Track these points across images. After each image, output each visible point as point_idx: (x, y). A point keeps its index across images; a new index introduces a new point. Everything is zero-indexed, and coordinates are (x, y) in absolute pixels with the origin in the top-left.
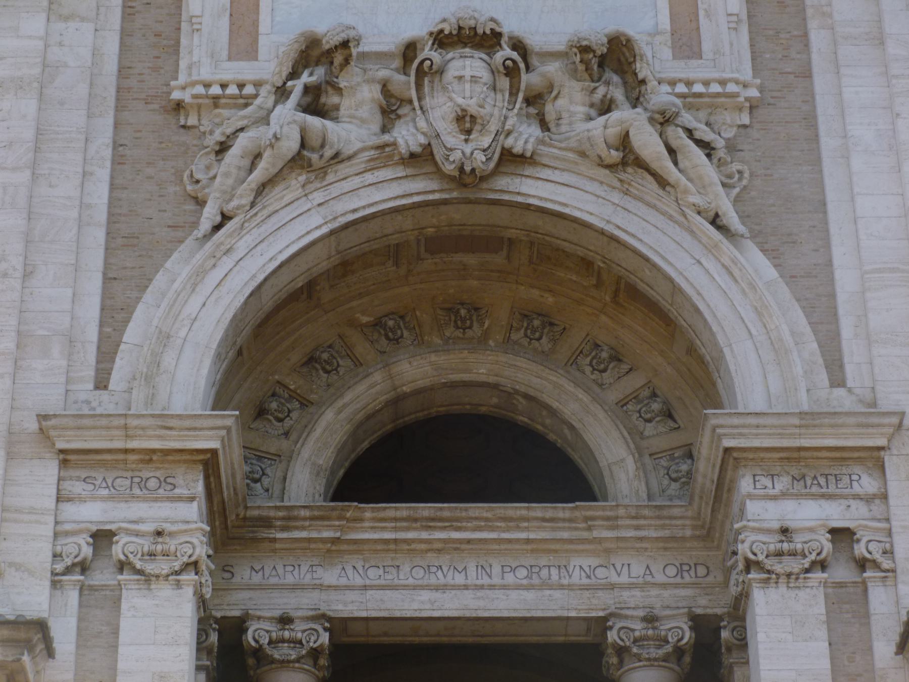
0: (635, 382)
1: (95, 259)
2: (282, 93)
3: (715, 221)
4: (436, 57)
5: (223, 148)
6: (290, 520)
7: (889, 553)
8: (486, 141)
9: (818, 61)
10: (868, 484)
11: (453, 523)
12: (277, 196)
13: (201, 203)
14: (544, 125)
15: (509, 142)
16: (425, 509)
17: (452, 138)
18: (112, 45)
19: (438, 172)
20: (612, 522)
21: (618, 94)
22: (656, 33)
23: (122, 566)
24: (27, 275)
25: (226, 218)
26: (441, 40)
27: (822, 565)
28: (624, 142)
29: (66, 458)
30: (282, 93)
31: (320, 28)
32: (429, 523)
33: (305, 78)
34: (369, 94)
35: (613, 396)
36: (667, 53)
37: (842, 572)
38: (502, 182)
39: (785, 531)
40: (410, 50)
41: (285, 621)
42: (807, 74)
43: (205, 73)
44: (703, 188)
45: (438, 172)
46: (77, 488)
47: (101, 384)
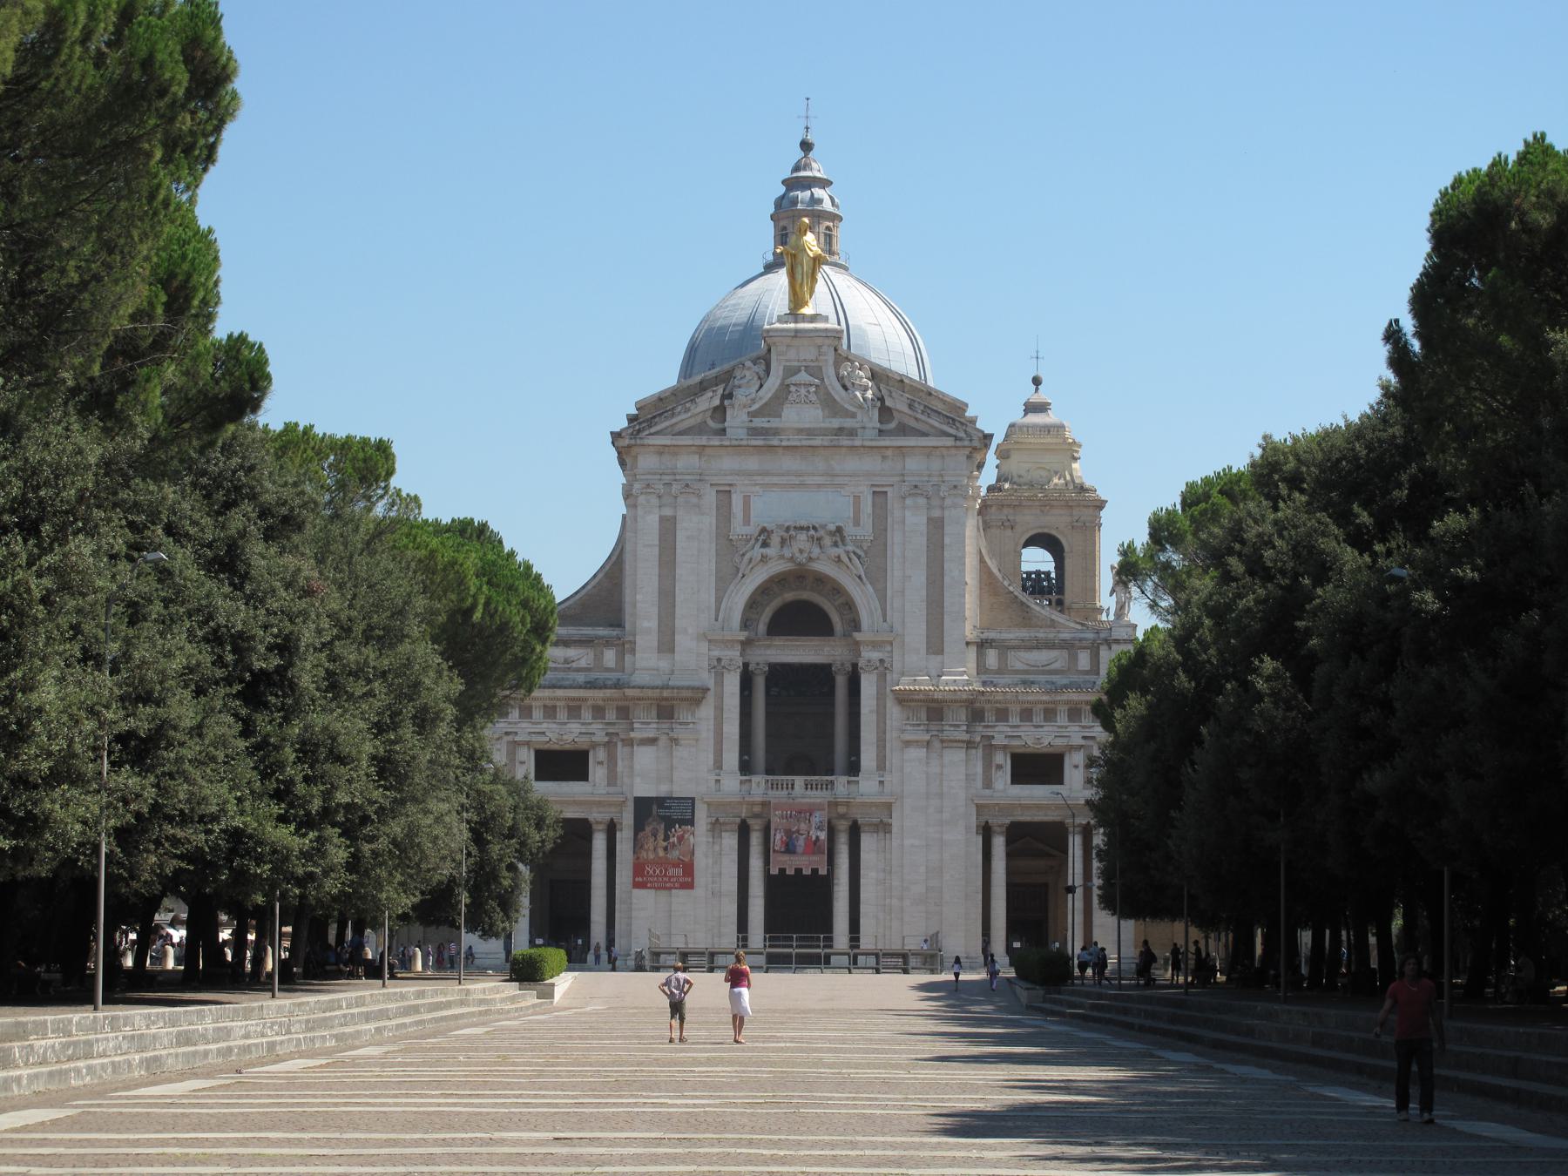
0: (842, 600)
1: (713, 585)
2: (757, 540)
3: (860, 577)
4: (794, 533)
5: (743, 555)
6: (759, 640)
7: (892, 666)
8: (806, 555)
10: (889, 648)
11: (796, 641)
13: (738, 570)
14: (821, 547)
15: (812, 556)
17: (797, 555)
18: (714, 521)
19: (794, 562)
20: (834, 641)
21: (838, 539)
22: (849, 518)
23: (724, 667)
24: (699, 591)
25: (743, 576)
26: (795, 527)
27: (877, 668)
28: (839, 557)
29: (710, 641)
30: (757, 540)
31: (765, 525)
32: (791, 640)
33: (762, 537)
35: (836, 603)
36: (851, 524)
37: (881, 669)
38: (810, 564)
39: (869, 661)
40: (788, 529)
41: (758, 664)
42: (886, 530)
43: (738, 530)
45: (794, 562)
46: (713, 647)
47: (716, 620)
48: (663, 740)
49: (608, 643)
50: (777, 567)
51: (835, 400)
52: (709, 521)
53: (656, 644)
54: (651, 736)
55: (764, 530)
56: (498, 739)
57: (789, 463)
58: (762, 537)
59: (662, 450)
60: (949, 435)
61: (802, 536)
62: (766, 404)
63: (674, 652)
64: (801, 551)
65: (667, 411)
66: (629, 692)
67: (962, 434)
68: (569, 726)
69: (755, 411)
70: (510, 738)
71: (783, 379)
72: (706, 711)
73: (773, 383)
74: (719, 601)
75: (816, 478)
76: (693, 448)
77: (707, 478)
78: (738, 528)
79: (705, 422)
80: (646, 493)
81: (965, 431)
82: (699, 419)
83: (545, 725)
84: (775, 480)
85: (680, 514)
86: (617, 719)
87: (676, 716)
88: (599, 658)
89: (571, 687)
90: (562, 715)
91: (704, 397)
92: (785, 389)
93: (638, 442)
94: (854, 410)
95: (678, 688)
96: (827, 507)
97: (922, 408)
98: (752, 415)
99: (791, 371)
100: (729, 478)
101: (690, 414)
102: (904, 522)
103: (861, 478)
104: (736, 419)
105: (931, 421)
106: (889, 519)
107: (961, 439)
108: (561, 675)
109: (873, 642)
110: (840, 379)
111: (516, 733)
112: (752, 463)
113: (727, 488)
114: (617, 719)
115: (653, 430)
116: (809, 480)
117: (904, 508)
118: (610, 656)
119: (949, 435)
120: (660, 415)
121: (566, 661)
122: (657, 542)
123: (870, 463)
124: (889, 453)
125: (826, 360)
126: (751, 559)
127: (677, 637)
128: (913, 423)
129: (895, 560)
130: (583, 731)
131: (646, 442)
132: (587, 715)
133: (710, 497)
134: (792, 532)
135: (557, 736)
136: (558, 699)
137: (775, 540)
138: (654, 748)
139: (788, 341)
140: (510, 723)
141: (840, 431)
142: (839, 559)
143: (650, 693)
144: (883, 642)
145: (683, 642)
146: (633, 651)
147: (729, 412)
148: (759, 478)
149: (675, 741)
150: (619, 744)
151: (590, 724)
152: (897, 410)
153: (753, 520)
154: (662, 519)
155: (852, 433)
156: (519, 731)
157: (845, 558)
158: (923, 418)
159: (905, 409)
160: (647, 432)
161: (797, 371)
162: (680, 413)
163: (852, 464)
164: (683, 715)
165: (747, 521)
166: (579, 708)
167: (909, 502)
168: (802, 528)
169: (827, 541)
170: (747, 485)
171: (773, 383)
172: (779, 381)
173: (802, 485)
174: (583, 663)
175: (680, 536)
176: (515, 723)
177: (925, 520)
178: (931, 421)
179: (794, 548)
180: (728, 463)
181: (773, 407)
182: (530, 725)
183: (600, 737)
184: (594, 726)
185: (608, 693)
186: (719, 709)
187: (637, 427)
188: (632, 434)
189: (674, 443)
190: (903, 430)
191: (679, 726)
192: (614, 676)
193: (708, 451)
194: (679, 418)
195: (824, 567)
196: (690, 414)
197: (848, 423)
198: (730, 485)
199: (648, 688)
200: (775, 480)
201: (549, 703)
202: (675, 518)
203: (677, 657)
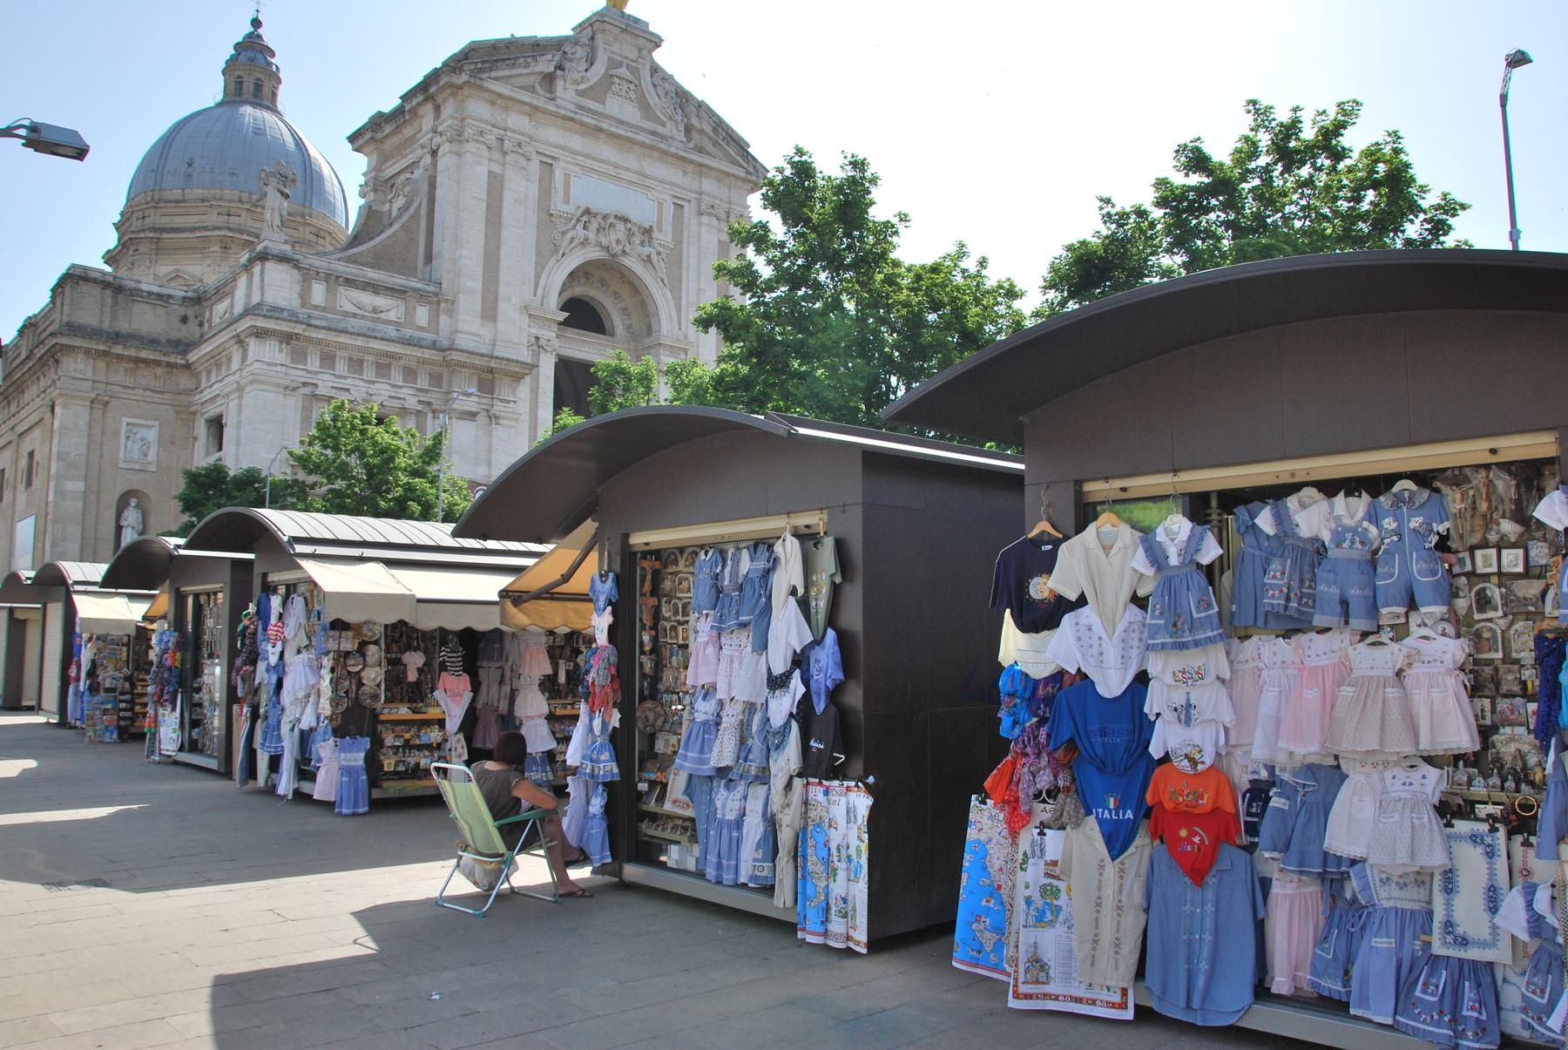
2: (578, 220)
5: (564, 233)
9: (685, 241)
11: (586, 336)
12: (576, 250)
16: (582, 332)
26: (616, 217)
28: (649, 256)
29: (530, 316)
30: (578, 220)
32: (581, 335)
33: (585, 218)
34: (596, 225)
38: (621, 258)
44: (662, 272)
45: (609, 252)
47: (535, 295)
48: (482, 418)
49: (422, 296)
50: (594, 254)
51: (649, 105)
52: (533, 190)
53: (479, 308)
54: (473, 409)
55: (587, 212)
56: (295, 389)
57: (606, 151)
58: (585, 218)
59: (497, 100)
60: (743, 167)
61: (621, 226)
62: (592, 87)
63: (495, 321)
64: (618, 241)
65: (507, 59)
66: (456, 356)
67: (751, 169)
68: (377, 386)
69: (583, 90)
70: (307, 390)
71: (607, 69)
72: (524, 390)
73: (599, 68)
74: (538, 276)
75: (631, 174)
76: (526, 108)
77: (534, 144)
78: (558, 205)
79: (533, 86)
80: (476, 141)
81: (754, 167)
82: (533, 79)
83: (349, 381)
84: (595, 165)
85: (509, 172)
86: (429, 385)
87: (497, 391)
88: (410, 313)
89: (382, 339)
90: (369, 373)
91: (544, 57)
92: (608, 79)
93: (478, 82)
94: (665, 120)
95: (508, 360)
96: (641, 208)
97: (724, 134)
98: (581, 93)
99: (614, 64)
100: (555, 150)
101: (528, 71)
102: (699, 240)
103: (667, 186)
104: (566, 92)
105: (728, 148)
106: (685, 233)
107: (750, 173)
108: (369, 324)
109: (671, 347)
110: (654, 86)
111: (316, 385)
112: (576, 142)
113: (549, 161)
114: (429, 385)
115: (493, 74)
116: (624, 174)
117: (700, 224)
118: (422, 314)
119: (743, 167)
120: (503, 60)
121: (375, 310)
122: (485, 198)
123: (672, 174)
124: (691, 168)
125: (644, 65)
126: (572, 239)
127: (501, 304)
128: (709, 147)
129: (690, 272)
130: (393, 394)
131: (485, 84)
132: (397, 377)
133: (535, 166)
134: (611, 220)
135: (364, 395)
136: (368, 351)
137: (594, 226)
138: (474, 423)
139: (617, 31)
140: (309, 372)
141: (654, 133)
142: (648, 259)
143: (477, 361)
144: (680, 349)
145: (509, 311)
146: (451, 313)
147: (560, 84)
148: (582, 158)
149: (493, 418)
150: (430, 415)
151: (401, 387)
152: (702, 132)
153: (571, 200)
154: (491, 174)
155: (663, 137)
156: (320, 383)
157: (654, 258)
158: (724, 145)
159: (711, 133)
160: (486, 75)
161: (620, 65)
162: (520, 66)
163: (659, 170)
164: (503, 391)
165: (567, 201)
166: (390, 366)
167: (705, 219)
168: (625, 220)
169: (637, 239)
170: (569, 163)
171: (599, 68)
172: (603, 70)
173: (617, 178)
174: (392, 316)
175: (508, 197)
176: (316, 373)
177: (716, 241)
178: (728, 148)
179: (613, 237)
180: (554, 135)
181: (599, 91)
182: (333, 378)
183: (412, 402)
184: (405, 390)
185: (427, 354)
186: (535, 392)
187: (479, 66)
188: (472, 71)
189: (513, 95)
190: (700, 150)
191: (499, 404)
192: (430, 336)
193: (539, 115)
194: (519, 71)
195: (633, 264)
196: (528, 71)
197: (660, 129)
198: (553, 158)
199: (477, 354)
200: (595, 165)
201: (355, 355)
202: (502, 176)
203: (500, 325)
